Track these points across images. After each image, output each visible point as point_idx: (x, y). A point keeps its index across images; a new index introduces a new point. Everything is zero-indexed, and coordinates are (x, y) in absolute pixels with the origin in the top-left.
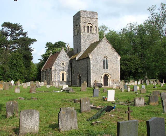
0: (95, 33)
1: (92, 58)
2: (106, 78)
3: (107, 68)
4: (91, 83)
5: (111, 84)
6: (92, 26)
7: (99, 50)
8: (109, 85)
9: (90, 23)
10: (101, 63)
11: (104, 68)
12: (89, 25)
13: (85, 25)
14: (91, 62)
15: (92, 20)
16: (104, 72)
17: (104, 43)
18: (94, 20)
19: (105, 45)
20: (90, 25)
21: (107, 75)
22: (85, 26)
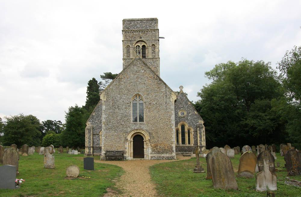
0: (151, 57)
1: (105, 100)
2: (138, 142)
3: (141, 119)
4: (102, 150)
5: (151, 154)
6: (146, 45)
7: (122, 83)
8: (145, 156)
9: (140, 39)
10: (126, 108)
11: (135, 120)
12: (139, 45)
13: (130, 45)
14: (104, 107)
15: (147, 34)
16: (133, 128)
17: (135, 68)
18: (150, 34)
19: (139, 72)
20: (141, 45)
21: (142, 135)
22: (131, 46)
